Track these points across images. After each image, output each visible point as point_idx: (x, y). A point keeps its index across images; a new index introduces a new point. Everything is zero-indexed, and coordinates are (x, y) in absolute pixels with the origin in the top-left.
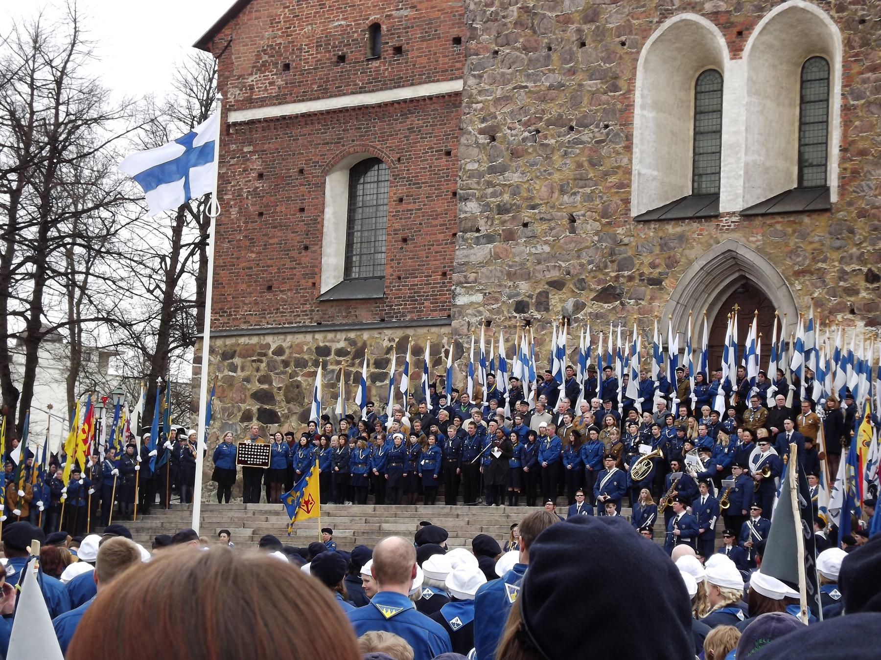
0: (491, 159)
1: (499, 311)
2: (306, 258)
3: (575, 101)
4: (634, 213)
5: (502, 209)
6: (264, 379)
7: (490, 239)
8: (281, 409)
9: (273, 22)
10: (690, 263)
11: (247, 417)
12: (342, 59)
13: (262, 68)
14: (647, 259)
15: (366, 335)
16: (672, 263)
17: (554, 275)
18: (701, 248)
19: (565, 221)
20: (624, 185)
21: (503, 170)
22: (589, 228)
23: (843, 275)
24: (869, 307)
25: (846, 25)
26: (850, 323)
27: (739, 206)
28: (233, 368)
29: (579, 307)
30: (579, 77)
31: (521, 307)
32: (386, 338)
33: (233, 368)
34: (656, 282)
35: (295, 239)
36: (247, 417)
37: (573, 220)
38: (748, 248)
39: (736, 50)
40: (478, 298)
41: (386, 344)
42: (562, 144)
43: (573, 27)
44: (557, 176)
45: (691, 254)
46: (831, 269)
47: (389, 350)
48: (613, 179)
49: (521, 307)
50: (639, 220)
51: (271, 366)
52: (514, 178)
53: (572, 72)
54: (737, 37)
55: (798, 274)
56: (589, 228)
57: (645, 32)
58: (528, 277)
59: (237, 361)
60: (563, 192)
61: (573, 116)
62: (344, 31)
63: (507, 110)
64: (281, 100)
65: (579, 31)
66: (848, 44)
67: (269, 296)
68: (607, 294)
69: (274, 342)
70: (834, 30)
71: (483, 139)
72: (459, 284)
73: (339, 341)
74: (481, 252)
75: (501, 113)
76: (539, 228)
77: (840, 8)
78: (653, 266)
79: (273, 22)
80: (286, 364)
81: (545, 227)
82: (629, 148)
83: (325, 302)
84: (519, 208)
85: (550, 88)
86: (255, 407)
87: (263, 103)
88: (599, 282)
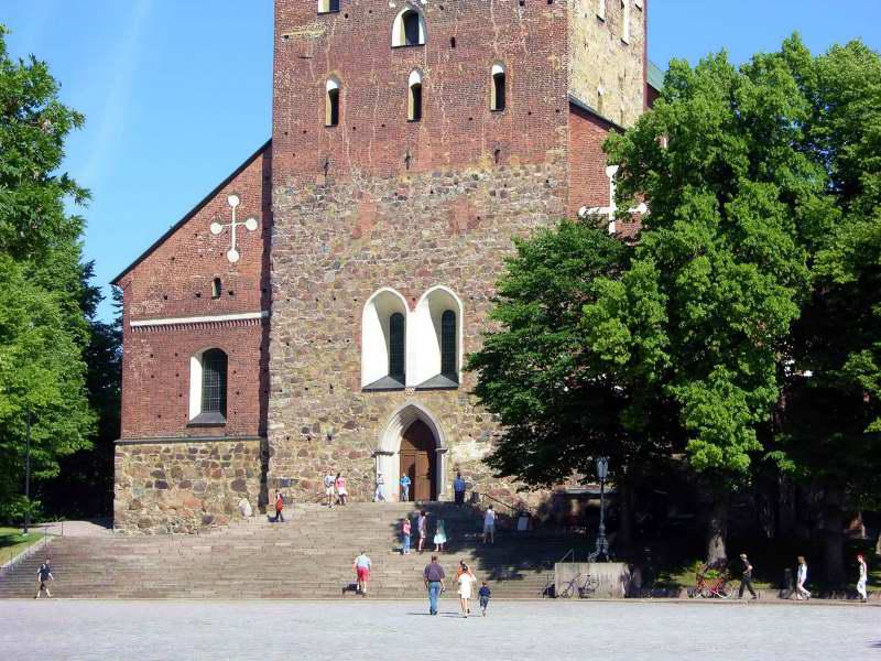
0: (287, 354)
1: (293, 432)
2: (180, 401)
3: (331, 329)
4: (365, 382)
5: (293, 381)
6: (160, 466)
7: (287, 395)
8: (169, 480)
9: (156, 273)
10: (392, 410)
11: (149, 485)
12: (199, 295)
13: (150, 297)
14: (370, 408)
15: (217, 443)
16: (383, 410)
17: (322, 415)
18: (397, 403)
19: (329, 388)
20: (358, 372)
21: (292, 361)
22: (340, 392)
23: (465, 418)
24: (478, 433)
25: (465, 299)
26: (470, 441)
27: (417, 383)
28: (140, 459)
29: (335, 431)
30: (334, 316)
31: (305, 431)
32: (229, 445)
33: (140, 459)
34: (375, 419)
35: (174, 390)
36: (149, 485)
37: (331, 387)
38: (422, 403)
39: (412, 308)
40: (282, 425)
41: (229, 448)
42: (323, 349)
43: (330, 290)
44: (323, 365)
45: (392, 406)
46: (459, 415)
47: (231, 450)
48: (352, 368)
49: (305, 431)
50: (364, 390)
51: (163, 458)
52: (299, 365)
53: (329, 312)
54: (414, 300)
55: (445, 417)
56: (340, 392)
57: (368, 294)
58: (308, 415)
59: (141, 455)
60: (326, 372)
61: (330, 335)
62: (200, 281)
63: (296, 329)
64: (162, 316)
65: (332, 293)
66: (465, 308)
67: (158, 420)
68: (350, 425)
69: (164, 446)
70: (459, 301)
71: (283, 345)
72: (272, 418)
73: (203, 446)
74: (282, 402)
75: (291, 330)
76: (313, 391)
77: (461, 291)
78: (373, 411)
79: (156, 273)
80: (172, 457)
81: (317, 390)
82: (360, 352)
83: (190, 426)
84: (302, 381)
85: (318, 320)
86: (154, 480)
87: (152, 317)
88: (346, 418)
